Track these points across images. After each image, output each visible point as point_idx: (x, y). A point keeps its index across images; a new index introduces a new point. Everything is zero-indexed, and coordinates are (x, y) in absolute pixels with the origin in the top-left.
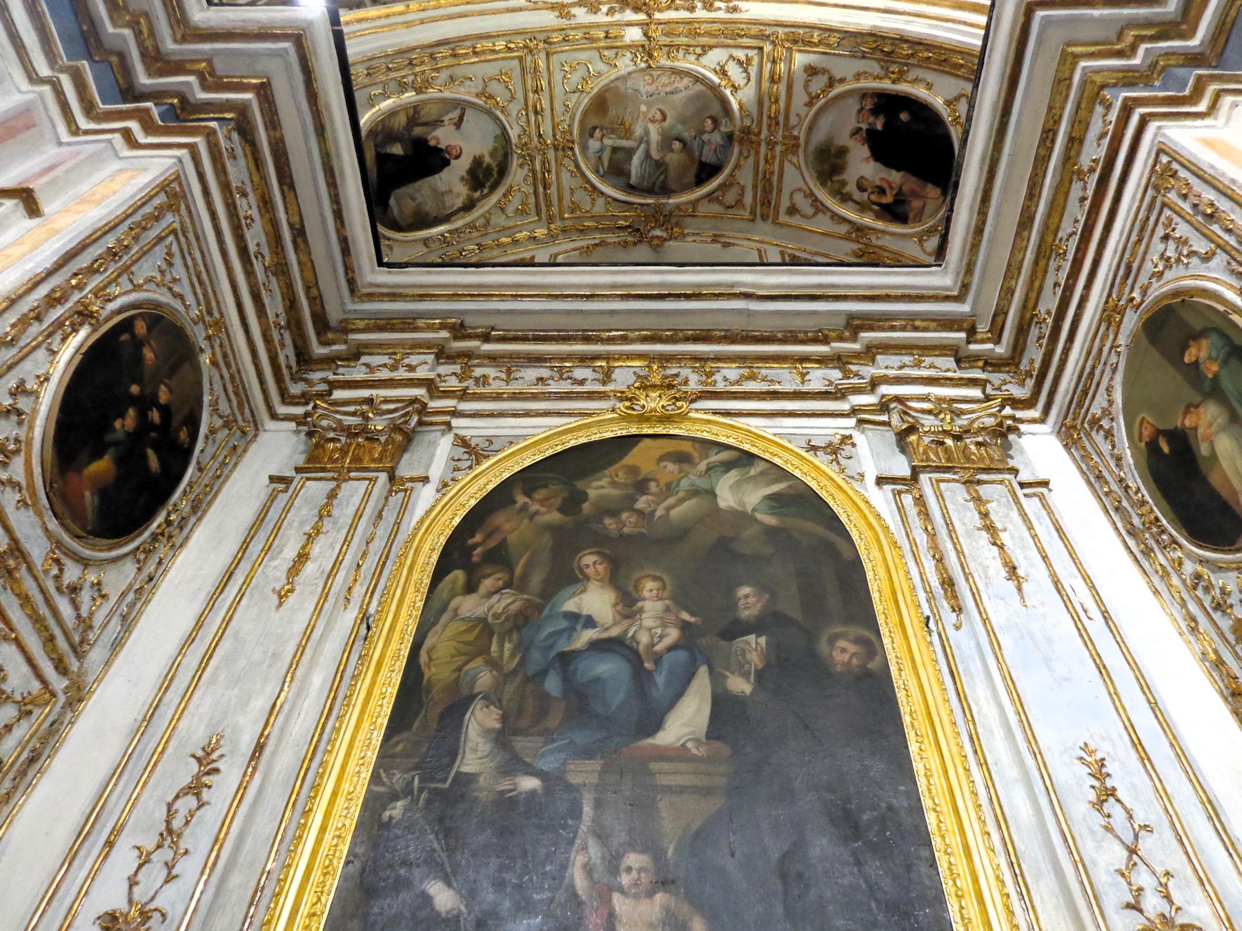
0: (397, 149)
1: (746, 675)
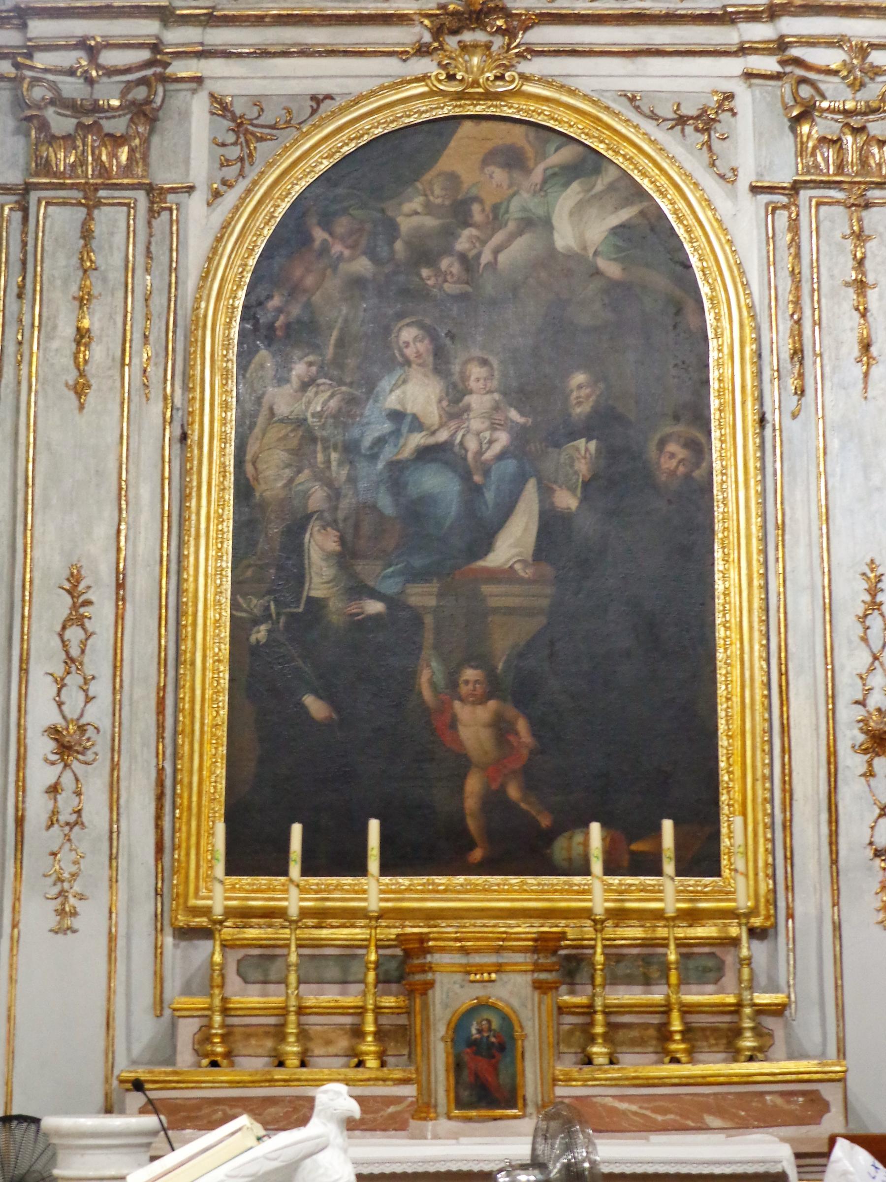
1: (572, 490)
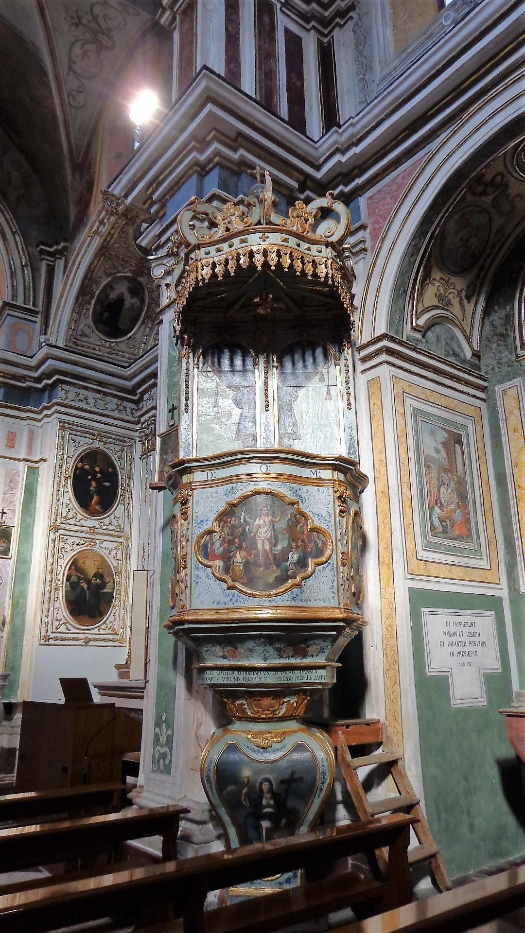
0: (106, 314)
